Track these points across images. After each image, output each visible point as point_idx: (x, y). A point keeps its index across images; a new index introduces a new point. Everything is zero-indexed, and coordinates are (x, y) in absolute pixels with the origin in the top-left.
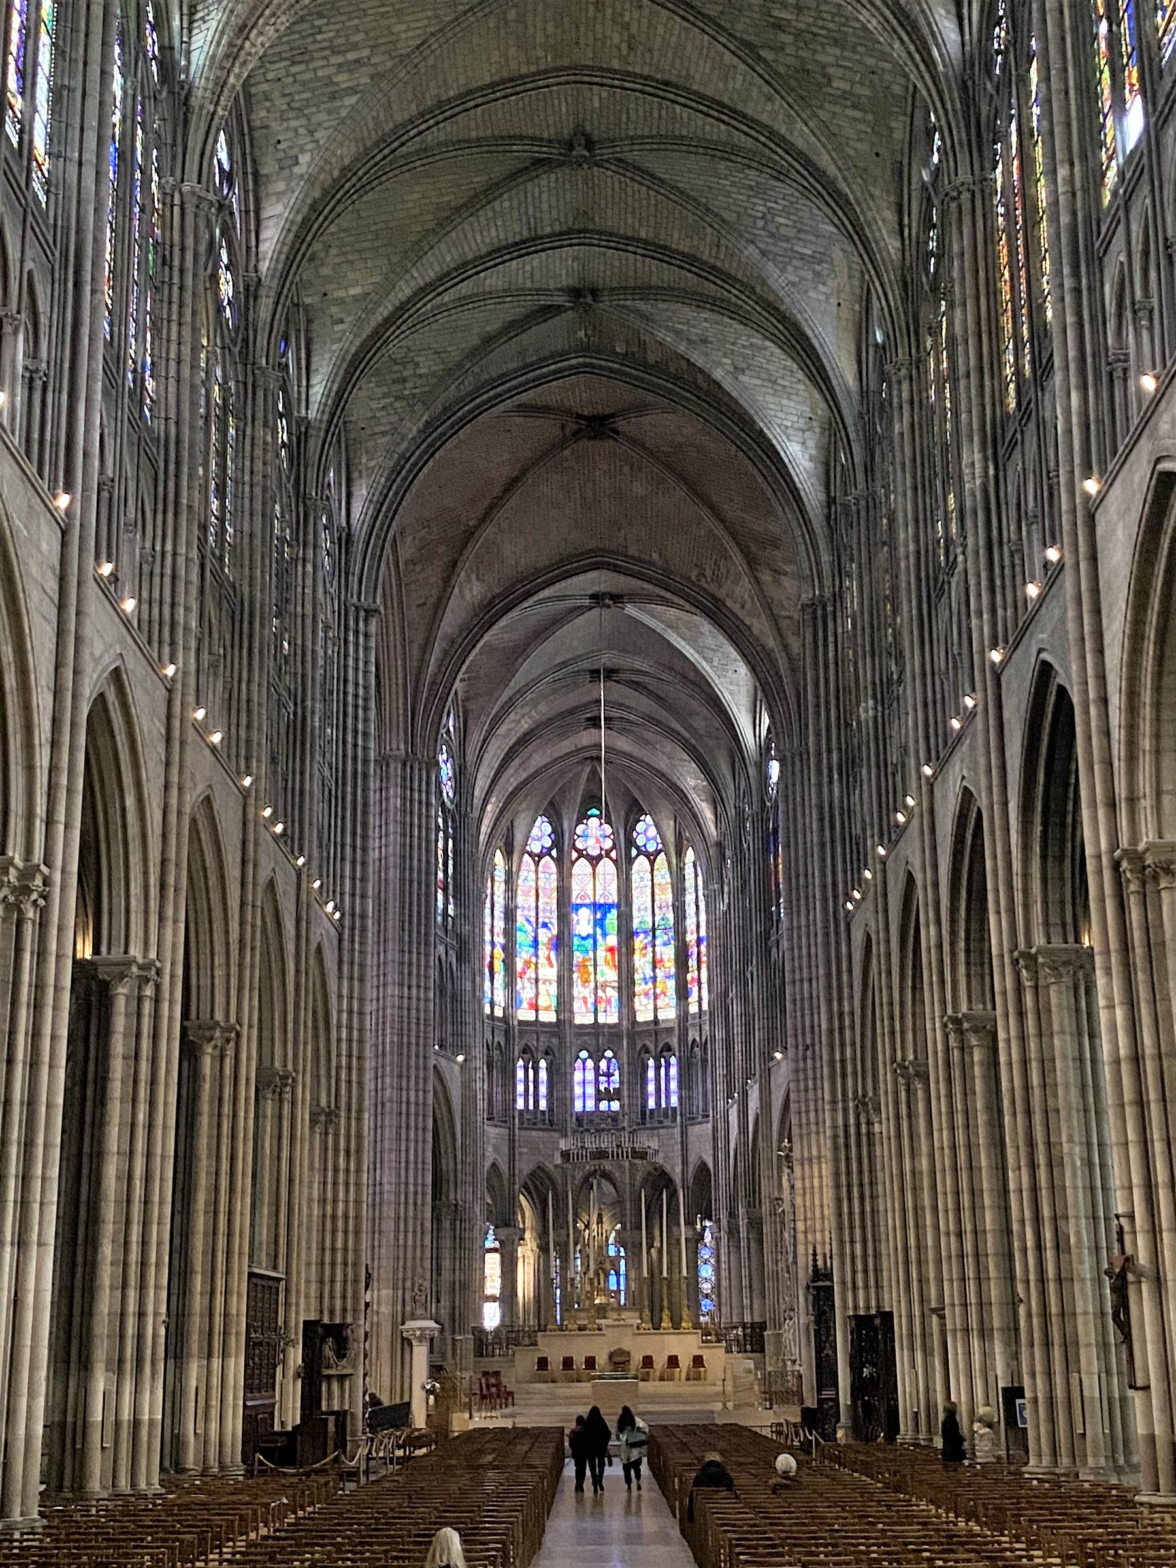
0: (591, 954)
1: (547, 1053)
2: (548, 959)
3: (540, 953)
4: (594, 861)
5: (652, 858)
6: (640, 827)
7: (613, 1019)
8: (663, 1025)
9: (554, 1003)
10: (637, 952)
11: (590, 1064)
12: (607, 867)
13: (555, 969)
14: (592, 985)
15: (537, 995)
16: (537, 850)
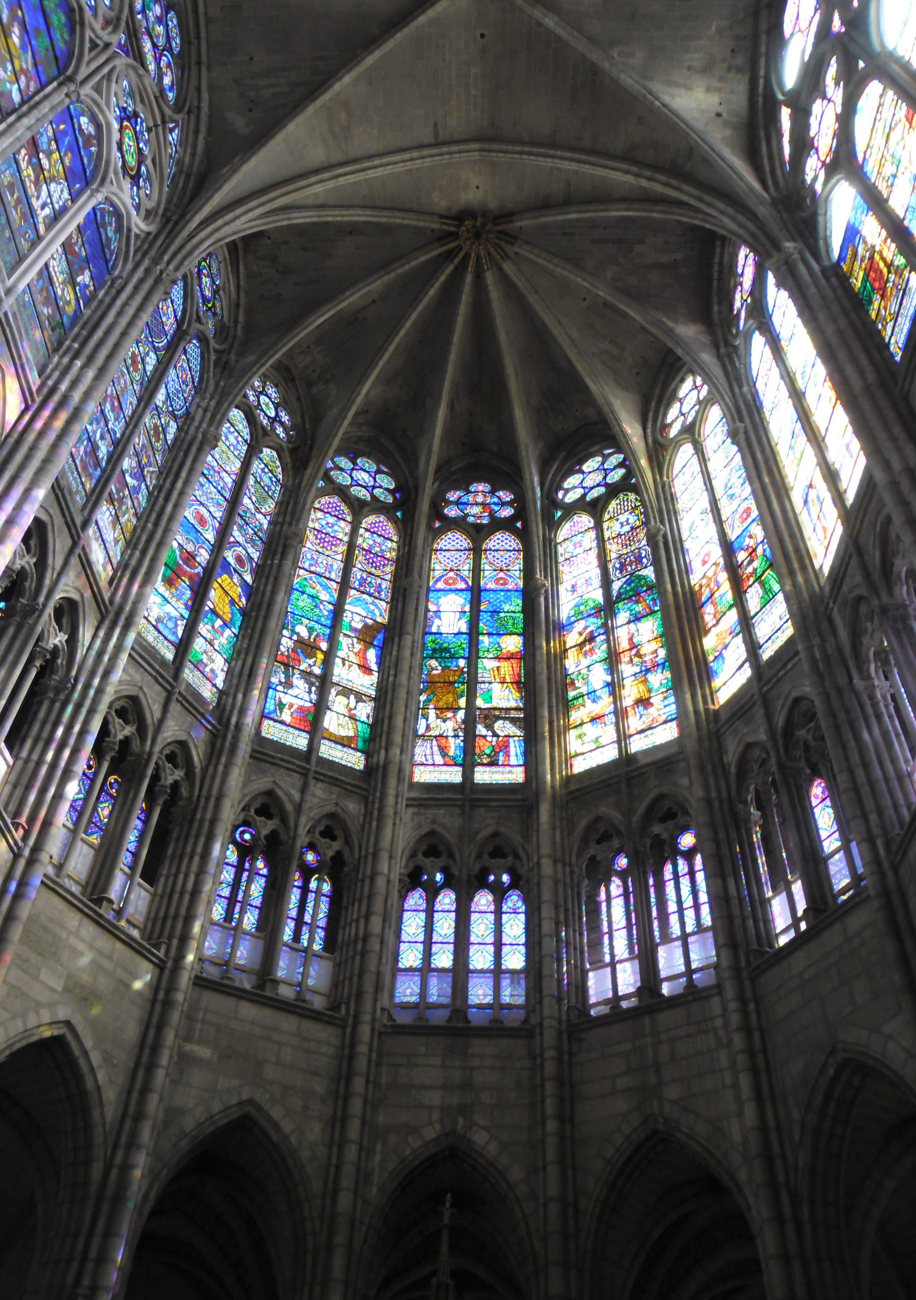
0: (462, 663)
1: (328, 833)
2: (363, 654)
3: (344, 642)
4: (478, 535)
5: (595, 508)
6: (572, 481)
7: (517, 776)
8: (643, 761)
9: (363, 730)
10: (572, 654)
11: (447, 900)
12: (502, 543)
13: (375, 677)
14: (461, 715)
15: (321, 706)
16: (363, 494)
